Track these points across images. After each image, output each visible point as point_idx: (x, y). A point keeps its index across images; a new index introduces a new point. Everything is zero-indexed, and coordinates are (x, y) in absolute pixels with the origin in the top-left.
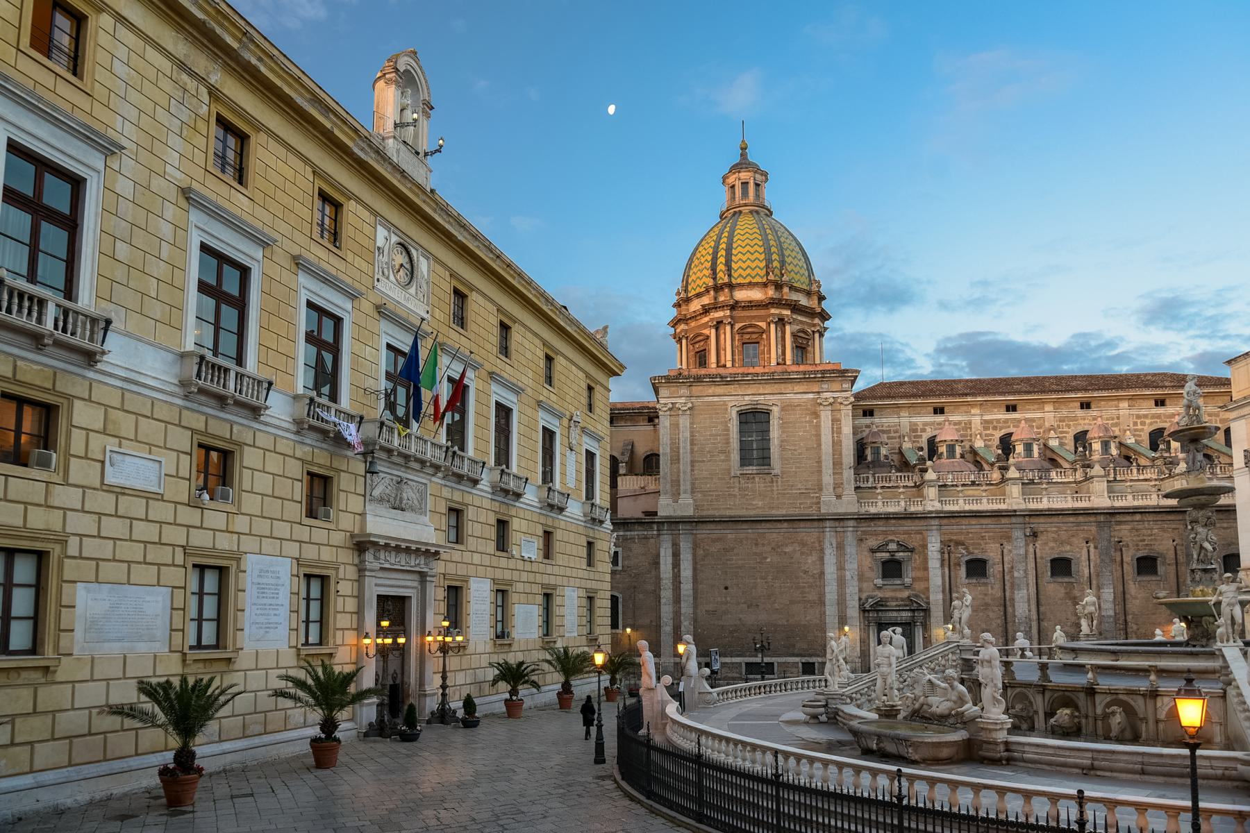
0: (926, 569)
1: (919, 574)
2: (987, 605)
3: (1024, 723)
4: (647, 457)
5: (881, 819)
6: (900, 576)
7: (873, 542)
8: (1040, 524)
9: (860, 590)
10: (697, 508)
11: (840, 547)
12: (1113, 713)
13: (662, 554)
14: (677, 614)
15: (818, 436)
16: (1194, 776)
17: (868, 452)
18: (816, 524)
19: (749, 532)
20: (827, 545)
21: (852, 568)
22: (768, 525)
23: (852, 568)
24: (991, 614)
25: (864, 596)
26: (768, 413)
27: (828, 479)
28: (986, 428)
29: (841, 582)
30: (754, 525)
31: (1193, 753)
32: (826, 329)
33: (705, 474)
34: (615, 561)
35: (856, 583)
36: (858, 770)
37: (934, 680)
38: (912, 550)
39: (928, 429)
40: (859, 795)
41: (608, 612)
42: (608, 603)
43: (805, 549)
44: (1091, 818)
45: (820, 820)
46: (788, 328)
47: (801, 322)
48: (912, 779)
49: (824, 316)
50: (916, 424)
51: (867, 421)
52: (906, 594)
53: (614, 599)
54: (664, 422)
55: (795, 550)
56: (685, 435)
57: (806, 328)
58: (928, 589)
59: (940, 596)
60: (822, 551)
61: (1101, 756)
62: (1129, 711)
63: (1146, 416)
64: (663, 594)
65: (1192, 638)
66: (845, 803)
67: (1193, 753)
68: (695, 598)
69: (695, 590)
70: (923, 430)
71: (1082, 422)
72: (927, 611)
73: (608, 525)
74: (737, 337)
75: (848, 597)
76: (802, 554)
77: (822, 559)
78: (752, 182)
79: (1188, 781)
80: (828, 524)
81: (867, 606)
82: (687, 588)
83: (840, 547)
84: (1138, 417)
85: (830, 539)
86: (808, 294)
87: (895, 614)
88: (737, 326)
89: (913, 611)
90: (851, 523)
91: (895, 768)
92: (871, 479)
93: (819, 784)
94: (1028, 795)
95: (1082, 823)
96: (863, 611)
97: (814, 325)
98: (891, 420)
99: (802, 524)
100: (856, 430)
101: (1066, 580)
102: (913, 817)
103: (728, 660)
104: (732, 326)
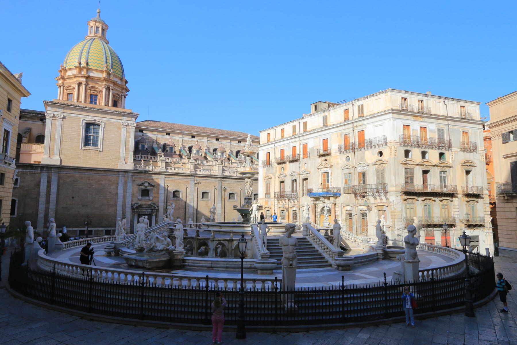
0: (158, 193)
1: (156, 195)
2: (179, 208)
3: (190, 251)
4: (38, 136)
5: (135, 293)
6: (148, 196)
7: (139, 182)
8: (199, 180)
9: (132, 201)
11: (125, 183)
12: (219, 247)
13: (42, 181)
14: (47, 209)
15: (120, 137)
16: (242, 268)
17: (140, 146)
18: (116, 173)
19: (87, 174)
20: (120, 182)
21: (129, 192)
22: (95, 172)
23: (129, 192)
24: (181, 212)
25: (133, 203)
26: (99, 125)
27: (122, 155)
29: (125, 197)
30: (88, 172)
31: (242, 260)
32: (127, 95)
34: (16, 183)
35: (130, 198)
36: (126, 274)
37: (160, 237)
38: (154, 186)
40: (126, 284)
41: (10, 207)
42: (10, 203)
44: (210, 286)
45: (109, 296)
47: (117, 90)
48: (148, 276)
49: (127, 90)
51: (141, 134)
52: (150, 203)
53: (13, 201)
54: (48, 121)
56: (58, 129)
57: (119, 93)
58: (158, 201)
59: (163, 204)
60: (118, 184)
61: (214, 263)
62: (223, 245)
63: (235, 146)
64: (40, 199)
65: (244, 221)
66: (120, 288)
67: (242, 260)
68: (57, 202)
69: (57, 198)
72: (158, 210)
73: (14, 166)
74: (89, 91)
75: (127, 203)
77: (117, 187)
78: (101, 27)
79: (240, 270)
80: (121, 173)
81: (134, 207)
82: (53, 197)
83: (125, 183)
85: (121, 179)
86: (121, 80)
87: (145, 211)
89: (152, 209)
90: (131, 174)
91: (142, 272)
92: (140, 157)
93: (110, 281)
94: (189, 279)
95: (207, 287)
96: (132, 208)
97: (122, 93)
99: (110, 173)
100: (136, 137)
101: (207, 200)
102: (147, 291)
103: (71, 229)
104: (86, 86)
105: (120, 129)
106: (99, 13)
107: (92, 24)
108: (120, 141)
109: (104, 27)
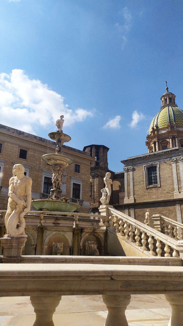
10: (135, 200)
15: (172, 172)
26: (156, 167)
27: (176, 186)
33: (137, 189)
43: (170, 212)
46: (176, 139)
55: (166, 213)
56: (131, 177)
76: (169, 214)
88: (160, 142)
105: (171, 165)
106: (167, 89)
107: (163, 99)
108: (172, 175)
109: (170, 96)
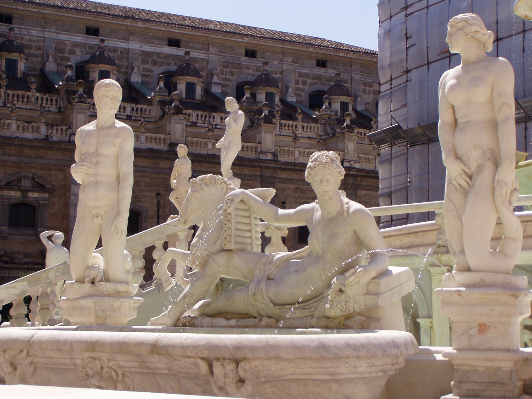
28: (145, 62)
39: (78, 52)
50: (63, 42)
63: (307, 76)
70: (72, 52)
71: (246, 71)
84: (300, 75)
98: (34, 33)
